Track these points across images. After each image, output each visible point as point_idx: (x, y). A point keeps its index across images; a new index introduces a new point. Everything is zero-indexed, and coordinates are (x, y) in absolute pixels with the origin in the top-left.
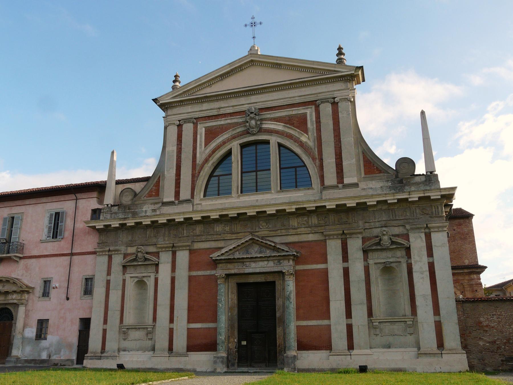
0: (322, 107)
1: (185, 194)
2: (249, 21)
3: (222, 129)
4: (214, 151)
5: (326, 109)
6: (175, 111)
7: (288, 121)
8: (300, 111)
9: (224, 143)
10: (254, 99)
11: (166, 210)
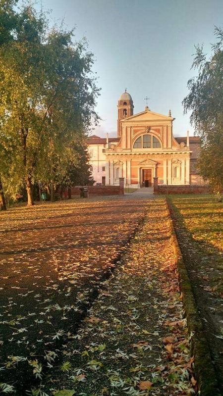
0: (164, 128)
1: (129, 147)
2: (146, 98)
3: (138, 131)
4: (136, 136)
5: (165, 128)
6: (125, 123)
7: (156, 130)
8: (159, 128)
9: (139, 134)
10: (147, 123)
11: (124, 151)
